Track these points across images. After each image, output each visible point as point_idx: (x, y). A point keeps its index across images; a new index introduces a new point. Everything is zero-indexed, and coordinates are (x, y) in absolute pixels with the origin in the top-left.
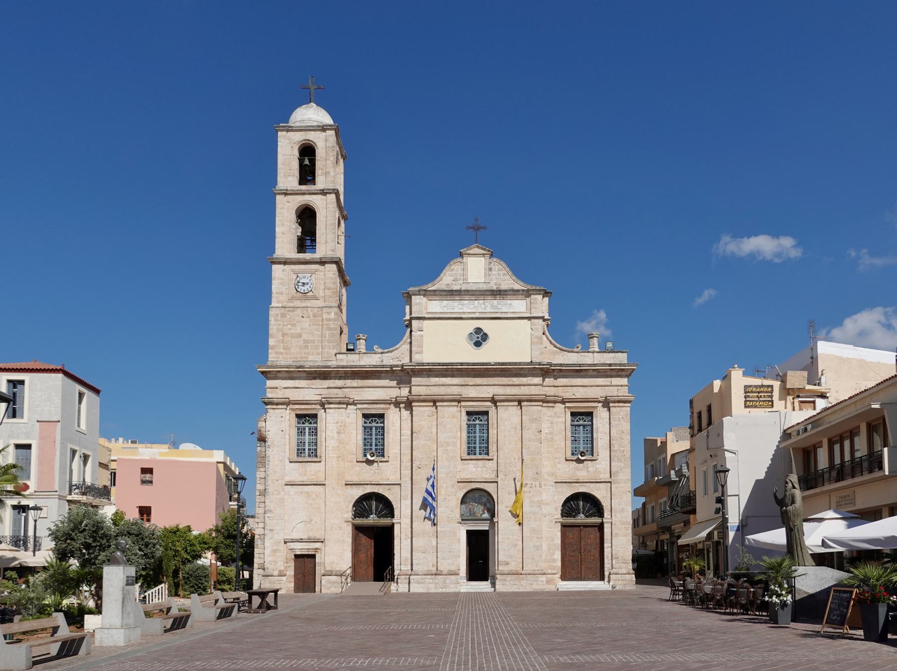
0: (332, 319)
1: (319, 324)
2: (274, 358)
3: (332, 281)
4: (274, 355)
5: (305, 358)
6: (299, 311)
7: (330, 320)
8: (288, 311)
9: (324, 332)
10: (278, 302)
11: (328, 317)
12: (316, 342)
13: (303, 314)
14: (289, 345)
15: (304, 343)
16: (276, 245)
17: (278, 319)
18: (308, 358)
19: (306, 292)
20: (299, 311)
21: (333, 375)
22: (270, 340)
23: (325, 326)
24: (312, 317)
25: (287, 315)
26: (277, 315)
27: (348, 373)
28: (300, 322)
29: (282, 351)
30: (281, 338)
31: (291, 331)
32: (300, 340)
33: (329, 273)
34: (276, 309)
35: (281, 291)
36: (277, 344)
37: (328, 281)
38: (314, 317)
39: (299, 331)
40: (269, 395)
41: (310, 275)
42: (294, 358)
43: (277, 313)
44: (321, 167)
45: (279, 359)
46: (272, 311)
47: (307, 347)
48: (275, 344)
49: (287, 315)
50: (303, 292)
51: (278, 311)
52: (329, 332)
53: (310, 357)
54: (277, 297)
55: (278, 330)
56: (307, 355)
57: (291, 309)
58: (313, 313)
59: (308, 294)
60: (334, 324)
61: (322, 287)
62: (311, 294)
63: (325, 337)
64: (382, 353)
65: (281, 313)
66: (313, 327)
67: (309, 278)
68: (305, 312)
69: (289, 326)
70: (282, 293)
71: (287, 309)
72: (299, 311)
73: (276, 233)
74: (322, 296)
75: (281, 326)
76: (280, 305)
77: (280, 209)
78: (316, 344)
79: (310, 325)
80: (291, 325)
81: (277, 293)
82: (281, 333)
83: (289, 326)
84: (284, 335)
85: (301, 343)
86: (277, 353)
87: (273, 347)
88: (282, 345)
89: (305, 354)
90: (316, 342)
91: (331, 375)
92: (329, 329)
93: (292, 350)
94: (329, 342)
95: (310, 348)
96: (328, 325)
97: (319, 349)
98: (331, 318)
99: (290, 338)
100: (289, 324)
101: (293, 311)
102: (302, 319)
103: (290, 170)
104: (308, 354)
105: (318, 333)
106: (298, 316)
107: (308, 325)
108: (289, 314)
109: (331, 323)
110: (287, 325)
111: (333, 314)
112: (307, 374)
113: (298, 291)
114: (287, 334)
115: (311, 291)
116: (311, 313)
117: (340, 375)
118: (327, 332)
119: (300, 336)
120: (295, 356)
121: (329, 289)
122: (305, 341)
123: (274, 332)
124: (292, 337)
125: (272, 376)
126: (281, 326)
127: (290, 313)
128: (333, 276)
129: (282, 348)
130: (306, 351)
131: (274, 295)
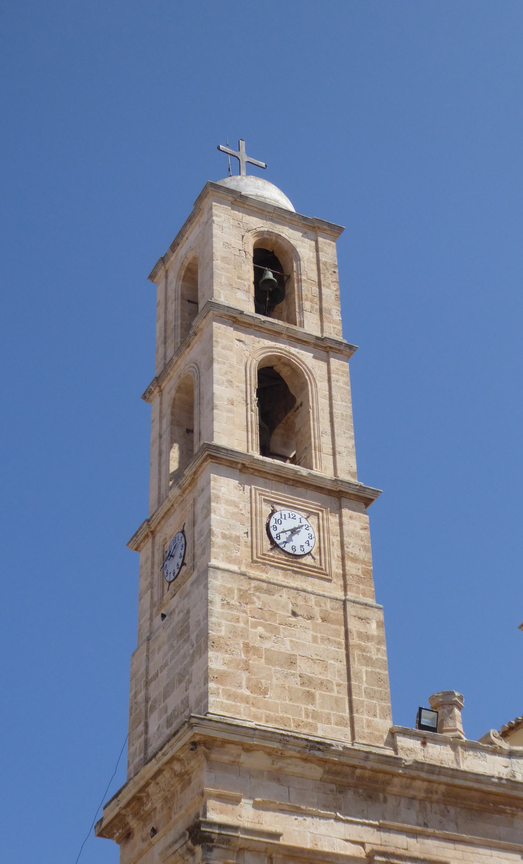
0: (373, 636)
1: (339, 643)
2: (223, 708)
3: (362, 543)
4: (222, 699)
5: (307, 725)
6: (285, 596)
7: (368, 638)
8: (258, 589)
9: (355, 666)
10: (229, 560)
11: (362, 630)
12: (335, 688)
13: (295, 605)
14: (263, 681)
15: (303, 684)
16: (215, 424)
17: (232, 602)
18: (316, 729)
19: (296, 553)
20: (284, 596)
21: (395, 790)
22: (211, 654)
23: (355, 653)
24: (320, 621)
25: (255, 599)
26: (230, 591)
27: (437, 793)
28: (290, 625)
29: (247, 693)
30: (243, 656)
31: (267, 645)
32: (293, 675)
33: (352, 521)
34: (226, 574)
35: (234, 533)
36: (230, 670)
37: (351, 541)
38: (324, 620)
39: (286, 648)
40: (213, 816)
41: (304, 515)
42: (276, 721)
43: (229, 586)
44: (310, 296)
45: (239, 713)
46: (215, 578)
47: (310, 697)
48: (224, 668)
49: (255, 599)
50: (291, 552)
51: (234, 584)
52: (369, 669)
53: (319, 725)
54: (225, 546)
55: (234, 632)
56: (313, 718)
57: (265, 585)
58: (321, 611)
59: (303, 560)
60: (378, 650)
61: (336, 552)
62: (308, 560)
63: (360, 679)
64: (511, 754)
65: (240, 590)
66: (323, 646)
67: (304, 522)
68: (300, 601)
69: (260, 630)
70: (237, 539)
71: (254, 583)
72: (285, 596)
73: (215, 398)
74: (337, 575)
75: (242, 625)
76: (234, 568)
77: (223, 348)
78: (335, 694)
79: (315, 639)
80: (264, 626)
81: (224, 536)
82: (241, 642)
83: (260, 630)
84: (248, 648)
85: (294, 683)
86: (230, 696)
87: (221, 678)
88: (244, 675)
89: (307, 716)
90: (335, 688)
91: (389, 788)
92: (368, 661)
93: (271, 697)
94: (370, 695)
95: (318, 701)
96: (364, 650)
97: (344, 712)
98: (369, 633)
99: (263, 660)
100: (260, 624)
101: (269, 592)
102: (293, 619)
103: (239, 278)
104: (315, 715)
105: (338, 665)
106: (284, 607)
107: (310, 639)
108: (259, 598)
109: (371, 646)
110: (255, 626)
111: (374, 625)
112: (327, 772)
113: (275, 545)
114: (256, 650)
115: (309, 553)
116: (317, 610)
117: (412, 793)
118: (364, 669)
119: (292, 662)
120: (281, 715)
121: (355, 560)
122: (306, 681)
123: (223, 634)
124: (269, 661)
125: (225, 758)
126: (242, 625)
127: (264, 597)
128: (362, 532)
129: (244, 684)
130: (310, 707)
131: (217, 540)
